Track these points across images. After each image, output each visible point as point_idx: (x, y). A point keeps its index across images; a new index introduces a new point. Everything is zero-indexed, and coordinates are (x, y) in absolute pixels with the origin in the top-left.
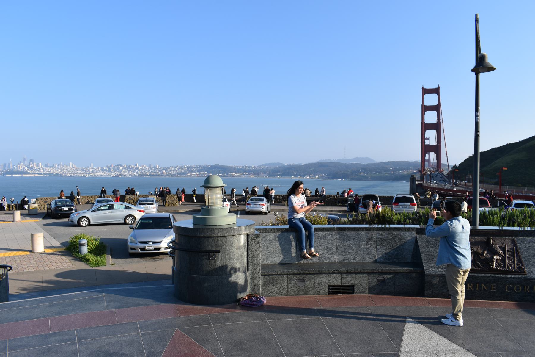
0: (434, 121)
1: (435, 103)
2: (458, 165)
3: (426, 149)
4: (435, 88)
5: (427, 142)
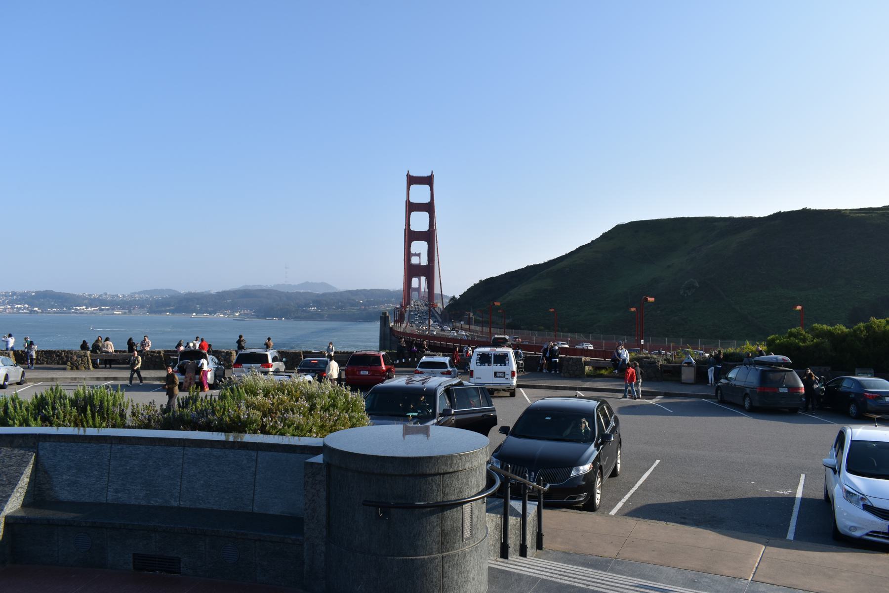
0: (425, 227)
1: (427, 200)
2: (457, 297)
3: (412, 271)
4: (426, 175)
5: (415, 260)
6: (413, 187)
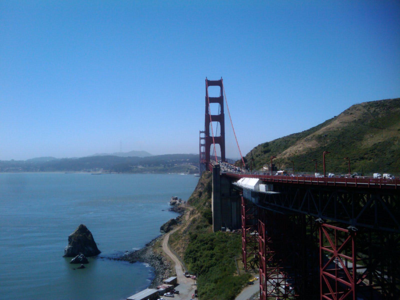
3: (209, 140)
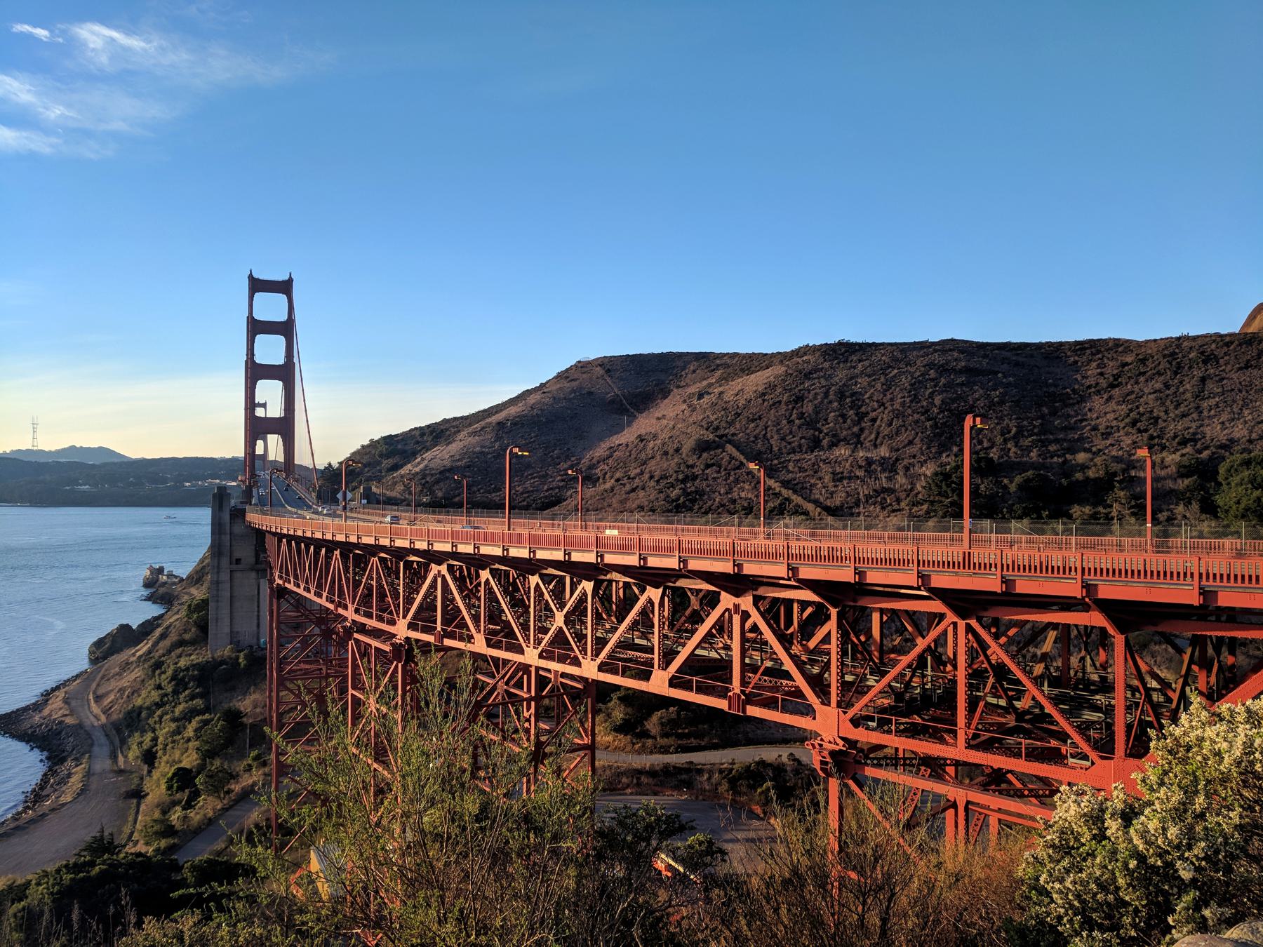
0: (279, 359)
1: (283, 317)
2: (335, 465)
3: (256, 428)
5: (260, 412)
6: (257, 295)
